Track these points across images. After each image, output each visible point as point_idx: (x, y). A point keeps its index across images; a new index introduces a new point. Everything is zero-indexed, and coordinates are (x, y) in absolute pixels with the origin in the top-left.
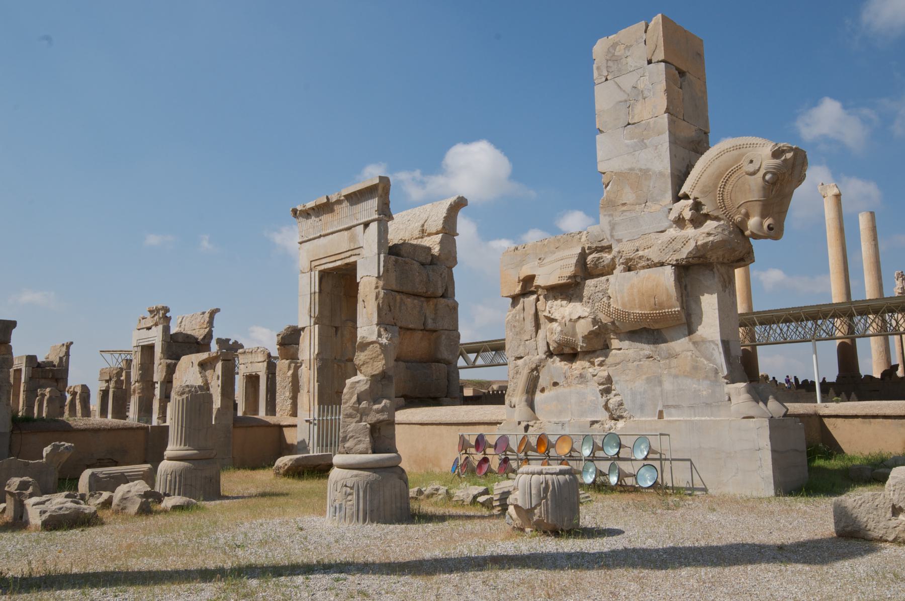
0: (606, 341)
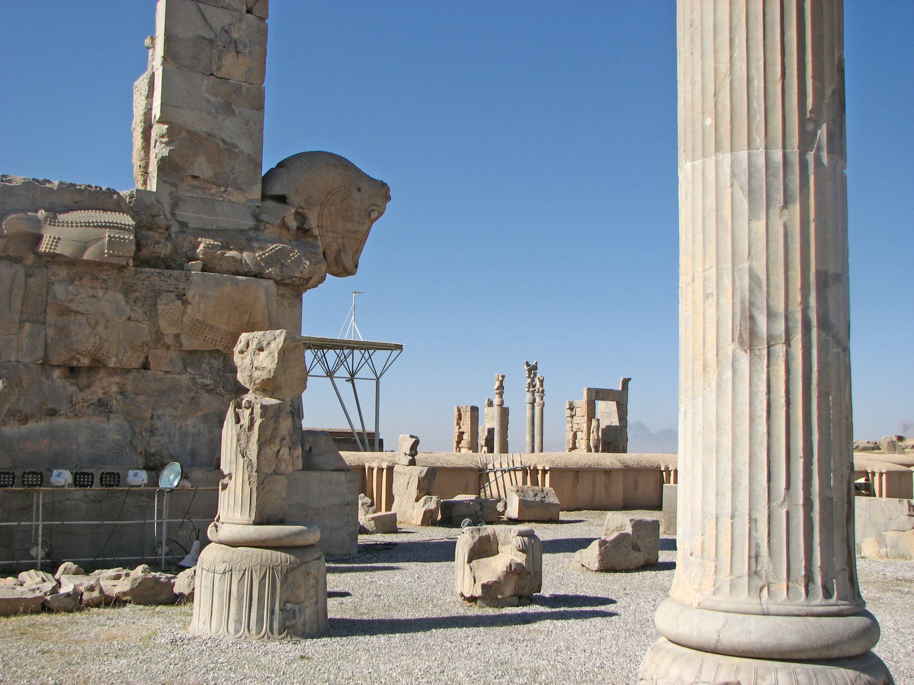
0: (147, 358)
